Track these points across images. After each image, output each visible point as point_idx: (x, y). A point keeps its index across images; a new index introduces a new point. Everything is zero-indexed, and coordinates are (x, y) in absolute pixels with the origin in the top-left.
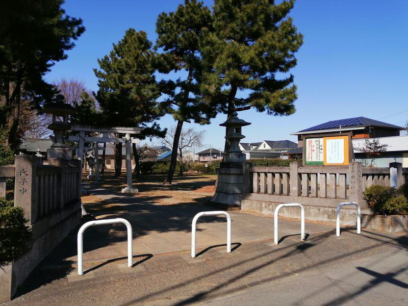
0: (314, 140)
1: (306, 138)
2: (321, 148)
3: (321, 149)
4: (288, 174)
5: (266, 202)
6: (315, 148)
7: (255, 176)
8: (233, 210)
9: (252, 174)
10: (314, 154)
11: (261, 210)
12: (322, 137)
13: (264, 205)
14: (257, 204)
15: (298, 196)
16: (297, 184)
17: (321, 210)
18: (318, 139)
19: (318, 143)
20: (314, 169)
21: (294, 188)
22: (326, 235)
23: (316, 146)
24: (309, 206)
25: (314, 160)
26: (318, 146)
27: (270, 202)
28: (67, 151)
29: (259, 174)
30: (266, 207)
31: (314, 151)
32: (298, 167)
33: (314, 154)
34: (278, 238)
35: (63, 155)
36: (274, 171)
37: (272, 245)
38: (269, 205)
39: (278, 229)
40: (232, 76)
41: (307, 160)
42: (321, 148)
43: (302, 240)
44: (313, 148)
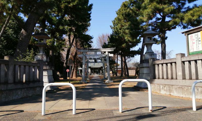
0: (193, 35)
1: (188, 35)
2: (199, 40)
3: (200, 41)
4: (175, 63)
5: (162, 85)
6: (195, 41)
7: (156, 66)
8: (143, 91)
9: (154, 65)
10: (195, 45)
11: (160, 91)
12: (199, 31)
13: (161, 87)
14: (157, 86)
15: (183, 79)
16: (181, 70)
17: (199, 90)
18: (197, 33)
19: (197, 36)
20: (193, 57)
21: (180, 73)
22: (184, 110)
23: (195, 39)
24: (190, 86)
25: (195, 50)
26: (197, 39)
27: (165, 84)
28: (44, 57)
29: (158, 65)
30: (162, 88)
31: (194, 43)
32: (181, 57)
33: (195, 45)
34: (72, 106)
35: (42, 59)
36: (167, 62)
37: (117, 112)
38: (164, 87)
39: (119, 101)
40: (153, 7)
41: (190, 51)
42: (199, 40)
43: (150, 111)
44: (194, 42)
